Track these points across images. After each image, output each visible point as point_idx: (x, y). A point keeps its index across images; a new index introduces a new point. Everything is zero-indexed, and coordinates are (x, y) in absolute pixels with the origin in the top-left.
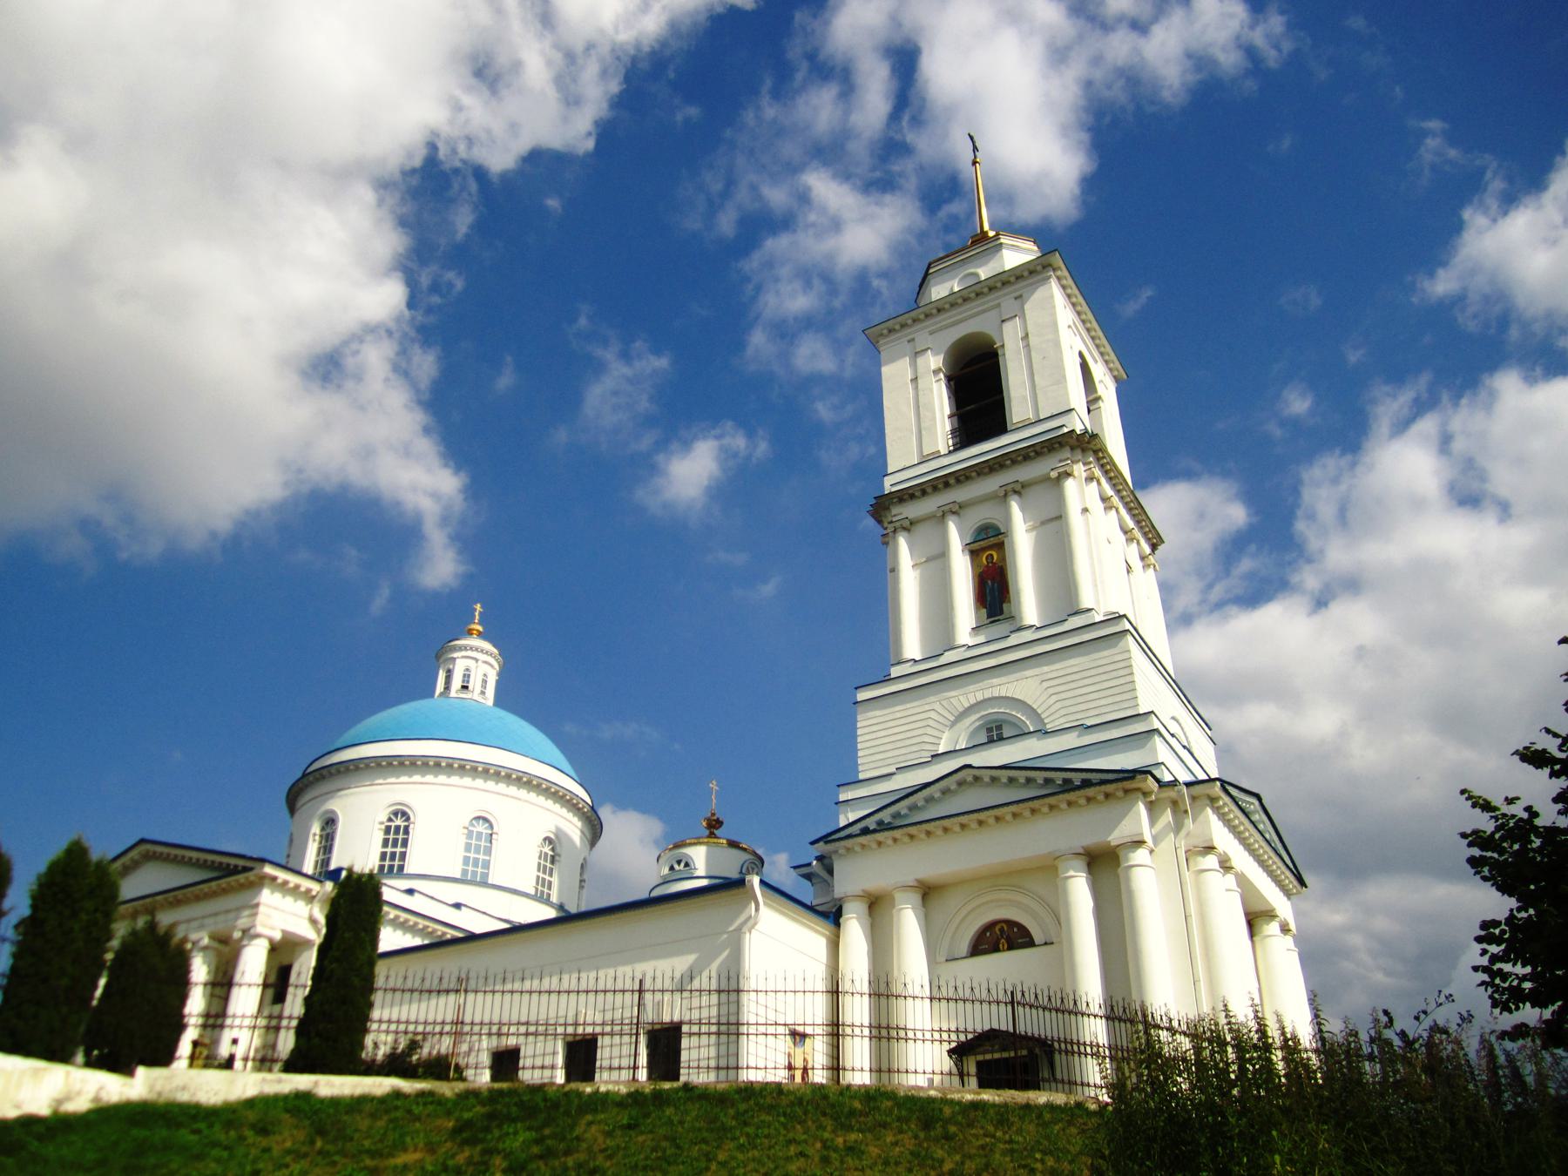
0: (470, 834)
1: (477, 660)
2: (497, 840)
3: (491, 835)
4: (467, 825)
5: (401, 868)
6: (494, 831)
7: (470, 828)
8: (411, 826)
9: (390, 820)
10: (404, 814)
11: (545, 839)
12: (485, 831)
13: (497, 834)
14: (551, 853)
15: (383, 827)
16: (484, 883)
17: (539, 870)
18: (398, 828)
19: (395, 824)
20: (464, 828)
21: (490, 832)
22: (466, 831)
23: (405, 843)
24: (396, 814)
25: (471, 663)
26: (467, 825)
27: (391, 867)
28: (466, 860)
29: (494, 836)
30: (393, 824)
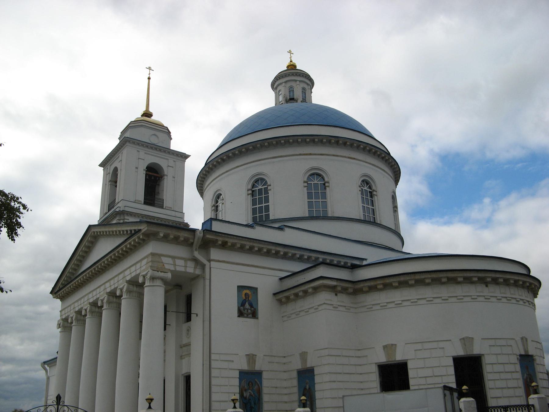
0: (309, 187)
1: (296, 81)
2: (328, 186)
3: (324, 184)
4: (306, 180)
5: (268, 216)
6: (326, 180)
7: (309, 182)
8: (269, 188)
9: (253, 186)
10: (262, 180)
11: (363, 181)
12: (319, 183)
13: (328, 182)
14: (369, 190)
15: (250, 192)
16: (326, 218)
17: (363, 203)
18: (260, 190)
19: (258, 188)
20: (305, 182)
21: (323, 182)
22: (306, 184)
23: (267, 200)
24: (257, 181)
25: (293, 84)
26: (306, 180)
27: (261, 217)
28: (310, 205)
29: (327, 184)
30: (257, 189)
